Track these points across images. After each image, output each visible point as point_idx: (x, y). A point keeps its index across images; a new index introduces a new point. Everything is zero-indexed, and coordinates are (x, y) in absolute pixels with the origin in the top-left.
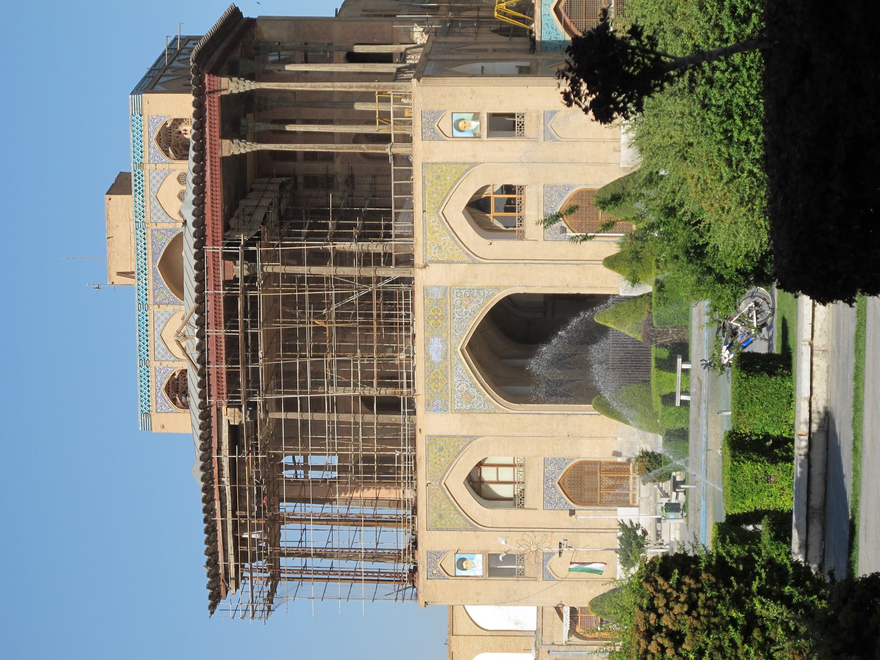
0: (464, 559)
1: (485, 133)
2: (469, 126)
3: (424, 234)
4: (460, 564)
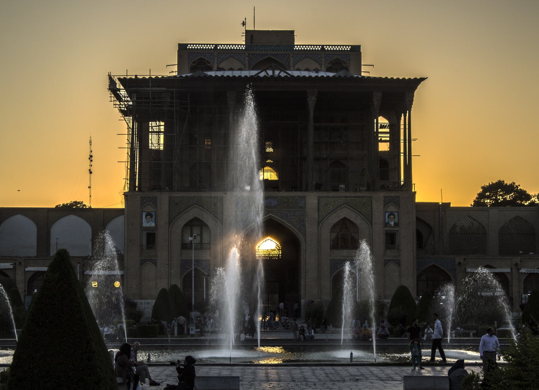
0: (152, 216)
1: (388, 229)
2: (391, 221)
3: (334, 197)
4: (149, 214)
